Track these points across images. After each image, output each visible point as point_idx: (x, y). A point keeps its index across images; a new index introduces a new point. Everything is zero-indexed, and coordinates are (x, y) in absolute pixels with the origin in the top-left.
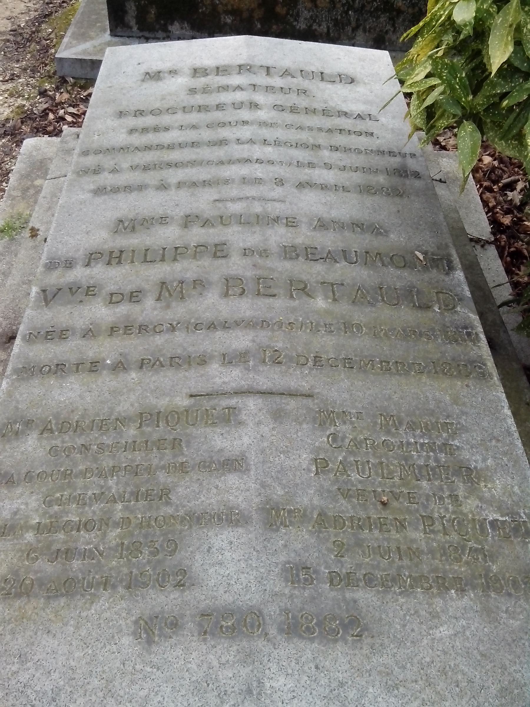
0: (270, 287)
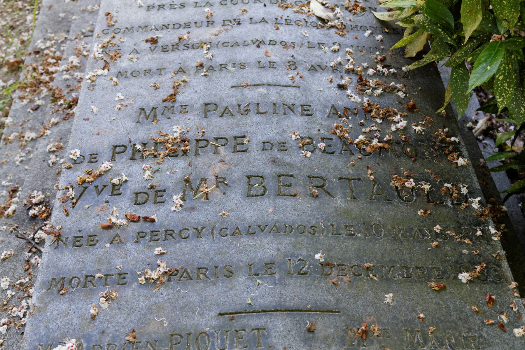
0: (290, 186)
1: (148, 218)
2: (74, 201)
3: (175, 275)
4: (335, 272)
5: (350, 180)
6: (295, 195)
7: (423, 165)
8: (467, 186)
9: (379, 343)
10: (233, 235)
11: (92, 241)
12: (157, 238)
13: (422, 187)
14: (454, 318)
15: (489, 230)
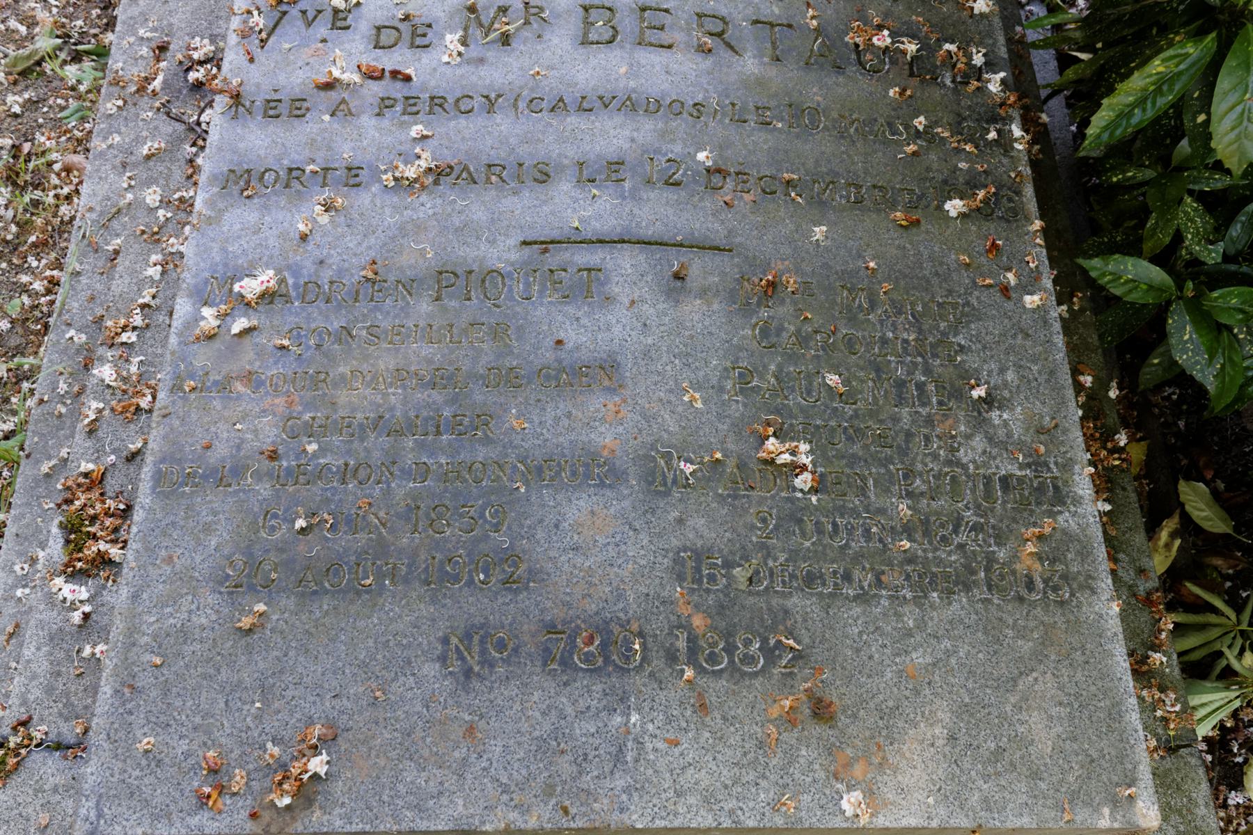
0: (662, 28)
1: (398, 72)
2: (264, 35)
3: (448, 175)
4: (730, 184)
5: (772, 25)
6: (670, 47)
7: (910, 8)
8: (984, 51)
9: (795, 303)
10: (552, 110)
11: (298, 109)
12: (414, 109)
13: (902, 47)
14: (927, 273)
15: (1010, 131)
